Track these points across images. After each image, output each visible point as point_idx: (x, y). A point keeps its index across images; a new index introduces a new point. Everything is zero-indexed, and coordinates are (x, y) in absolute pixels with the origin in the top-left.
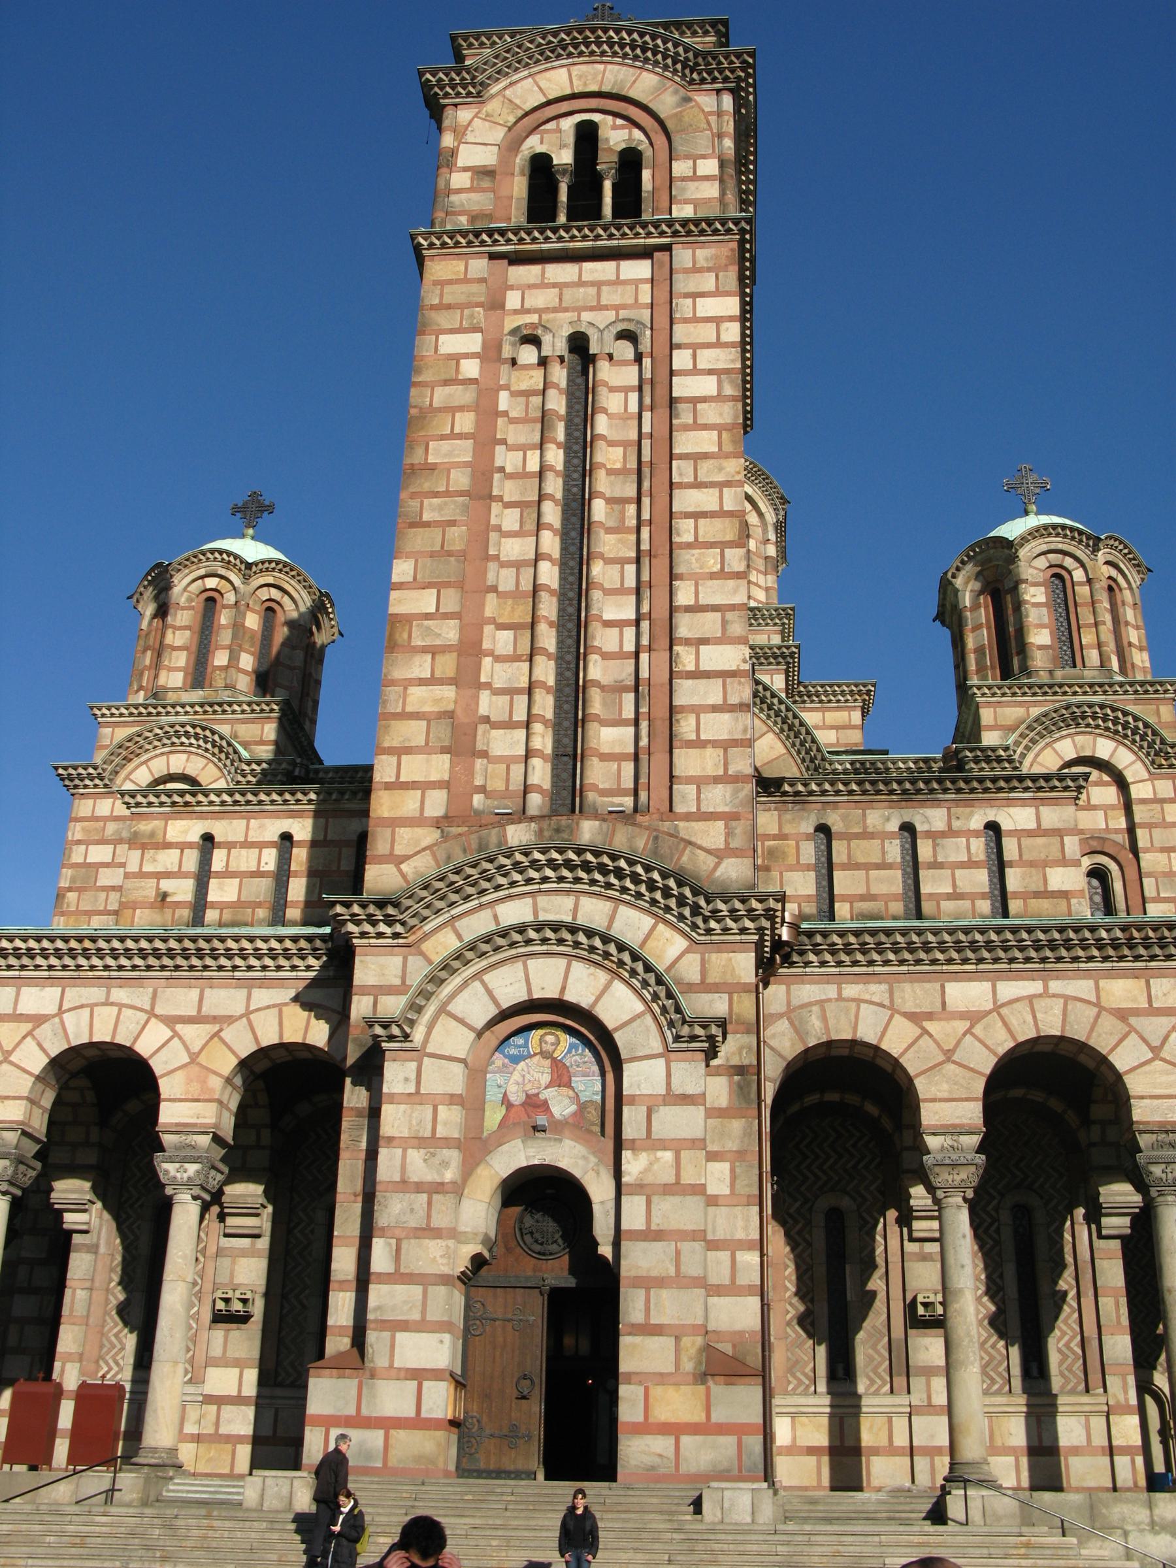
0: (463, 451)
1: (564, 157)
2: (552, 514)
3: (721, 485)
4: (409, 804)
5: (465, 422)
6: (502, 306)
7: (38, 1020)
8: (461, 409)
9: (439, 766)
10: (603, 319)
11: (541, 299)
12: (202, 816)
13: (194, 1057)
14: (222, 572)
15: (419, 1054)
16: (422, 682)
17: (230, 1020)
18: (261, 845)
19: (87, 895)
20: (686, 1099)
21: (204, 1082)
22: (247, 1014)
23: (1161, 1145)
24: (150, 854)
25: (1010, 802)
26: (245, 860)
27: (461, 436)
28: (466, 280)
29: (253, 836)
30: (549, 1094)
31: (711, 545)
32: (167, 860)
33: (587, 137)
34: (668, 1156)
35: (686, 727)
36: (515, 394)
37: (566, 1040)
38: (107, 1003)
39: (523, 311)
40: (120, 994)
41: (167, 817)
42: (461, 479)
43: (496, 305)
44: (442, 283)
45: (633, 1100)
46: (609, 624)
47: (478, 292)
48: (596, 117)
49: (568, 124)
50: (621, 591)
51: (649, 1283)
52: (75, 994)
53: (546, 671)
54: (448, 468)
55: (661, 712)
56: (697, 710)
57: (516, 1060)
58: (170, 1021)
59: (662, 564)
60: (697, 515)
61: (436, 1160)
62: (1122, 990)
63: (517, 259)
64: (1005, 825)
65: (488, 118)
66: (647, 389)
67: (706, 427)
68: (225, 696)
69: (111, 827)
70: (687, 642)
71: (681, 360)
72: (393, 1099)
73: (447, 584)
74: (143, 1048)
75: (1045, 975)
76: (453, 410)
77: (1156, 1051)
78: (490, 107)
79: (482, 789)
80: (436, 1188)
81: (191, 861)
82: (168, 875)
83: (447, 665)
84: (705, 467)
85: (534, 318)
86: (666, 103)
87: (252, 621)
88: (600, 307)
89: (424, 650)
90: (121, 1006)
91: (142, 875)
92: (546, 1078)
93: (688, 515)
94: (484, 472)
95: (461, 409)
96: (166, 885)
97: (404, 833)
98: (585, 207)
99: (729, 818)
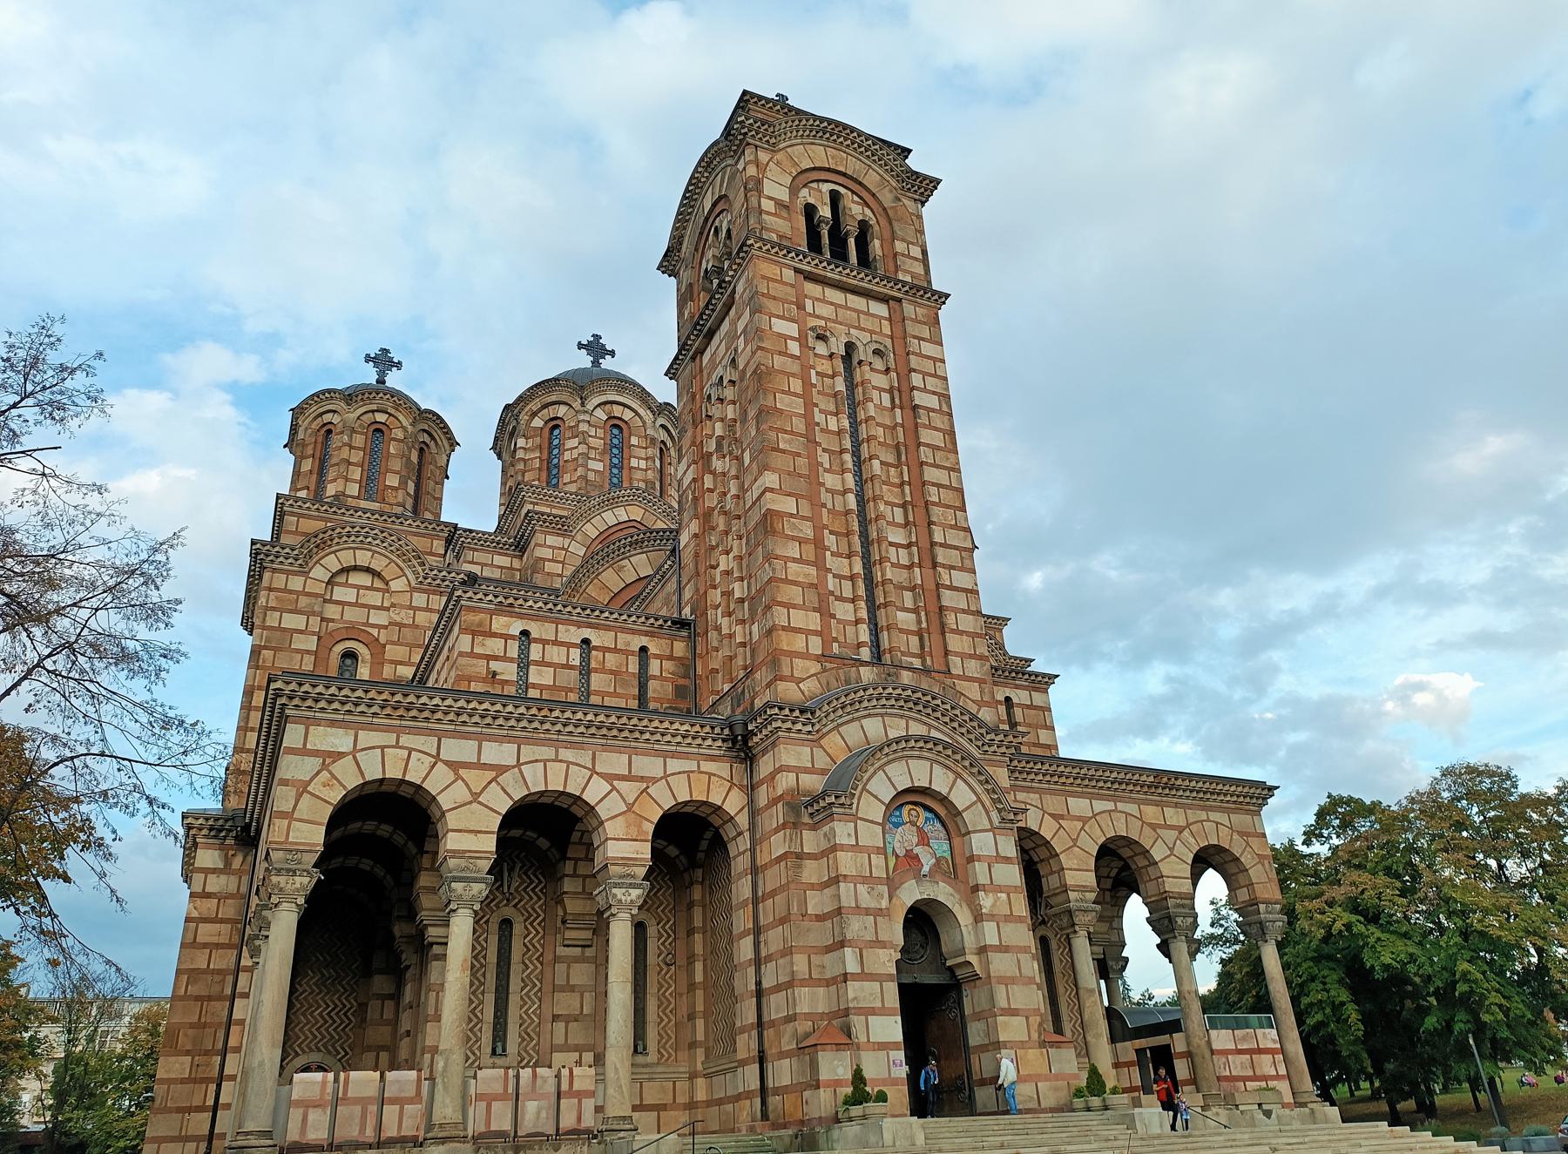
0: (798, 406)
1: (825, 211)
4: (799, 643)
5: (796, 385)
7: (501, 769)
8: (793, 375)
9: (814, 621)
12: (521, 616)
13: (630, 807)
14: (392, 411)
15: (855, 818)
16: (794, 560)
17: (655, 780)
18: (569, 645)
19: (279, 655)
20: (1007, 860)
21: (640, 826)
22: (665, 776)
23: (1179, 906)
24: (479, 639)
25: (1017, 687)
26: (556, 655)
27: (796, 395)
28: (781, 282)
29: (562, 637)
30: (918, 850)
31: (948, 507)
32: (495, 646)
34: (1004, 896)
35: (950, 619)
37: (923, 814)
38: (556, 760)
40: (566, 754)
41: (492, 613)
42: (799, 425)
43: (801, 307)
44: (769, 279)
45: (979, 859)
46: (891, 544)
47: (791, 294)
48: (842, 190)
50: (893, 524)
51: (1007, 981)
52: (528, 752)
53: (858, 568)
54: (792, 415)
55: (933, 608)
56: (956, 611)
57: (897, 825)
58: (610, 778)
59: (921, 511)
60: (939, 486)
61: (875, 893)
62: (1151, 812)
63: (810, 277)
64: (1015, 700)
65: (778, 164)
66: (896, 393)
67: (936, 429)
68: (399, 510)
69: (303, 602)
70: (944, 566)
71: (916, 379)
72: (843, 848)
73: (802, 497)
74: (590, 797)
75: (1114, 799)
76: (789, 375)
77: (1171, 849)
78: (779, 156)
79: (835, 640)
80: (878, 913)
81: (513, 651)
82: (496, 658)
83: (809, 552)
84: (939, 454)
85: (823, 323)
86: (887, 198)
87: (414, 457)
89: (793, 538)
90: (569, 763)
91: (472, 655)
92: (915, 840)
93: (934, 484)
94: (811, 424)
95: (793, 375)
96: (494, 665)
97: (796, 661)
98: (839, 254)
99: (981, 681)
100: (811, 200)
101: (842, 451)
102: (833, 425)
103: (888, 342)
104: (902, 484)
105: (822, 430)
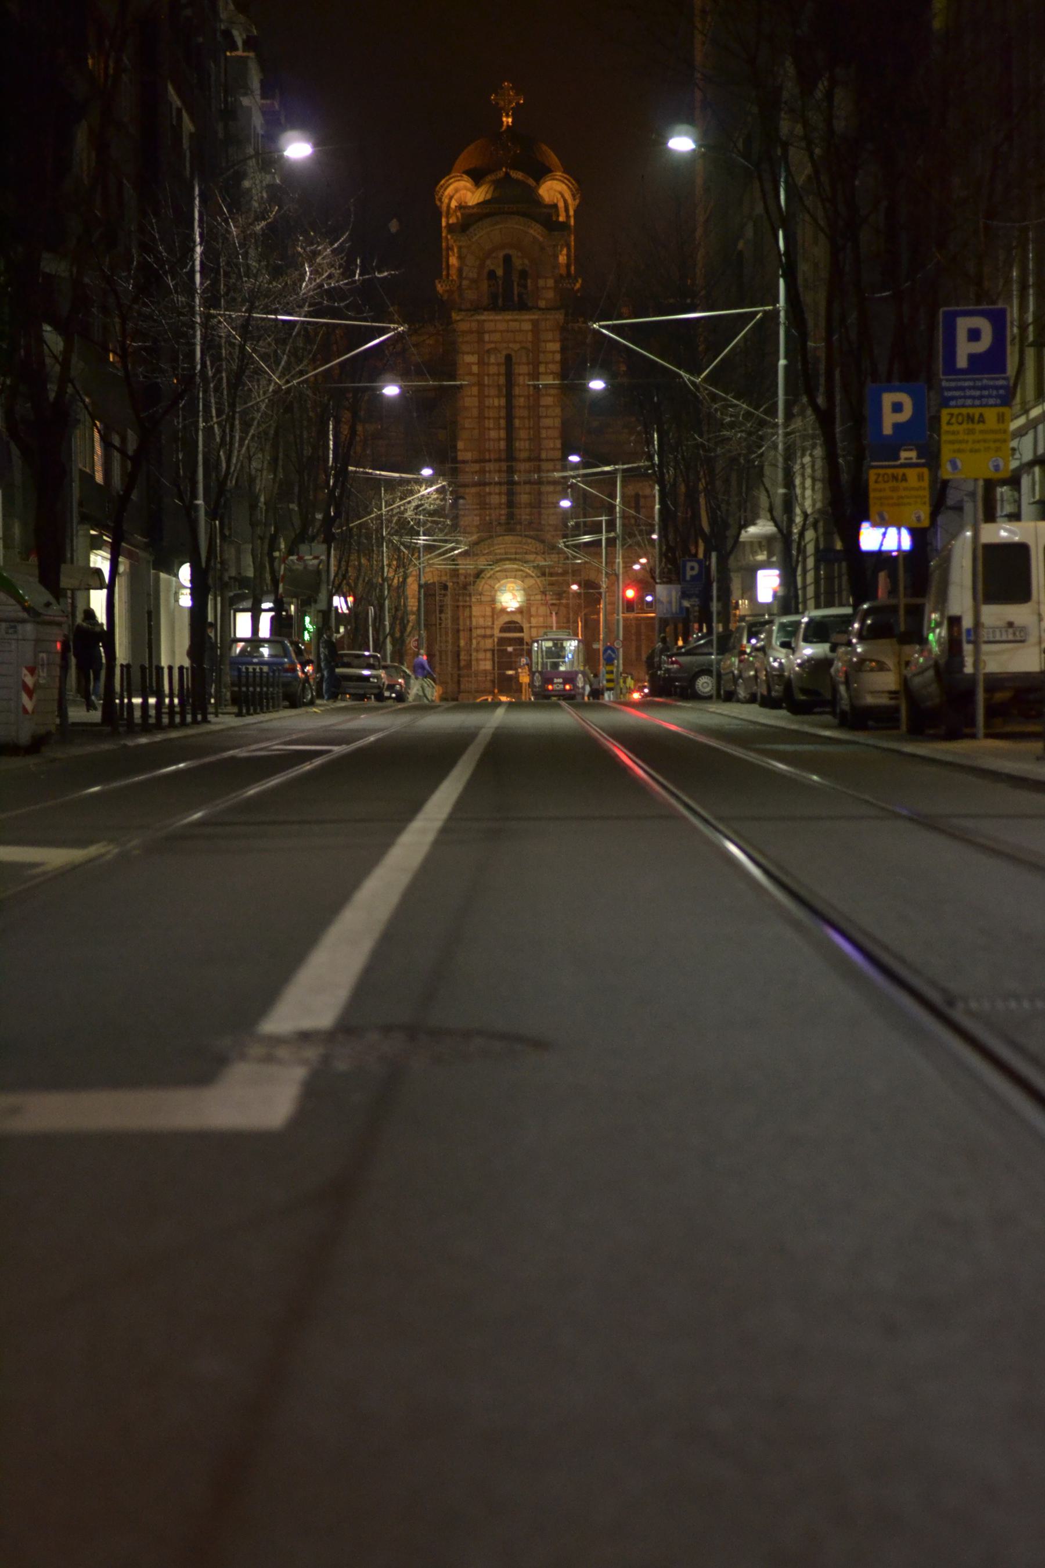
1: (500, 272)
2: (503, 422)
3: (554, 417)
5: (475, 390)
6: (484, 342)
10: (516, 346)
11: (497, 337)
33: (507, 259)
36: (488, 375)
39: (490, 342)
42: (475, 412)
49: (501, 254)
85: (493, 345)
88: (515, 342)
100: (492, 268)
101: (500, 417)
102: (496, 404)
103: (530, 346)
104: (529, 428)
105: (489, 407)
